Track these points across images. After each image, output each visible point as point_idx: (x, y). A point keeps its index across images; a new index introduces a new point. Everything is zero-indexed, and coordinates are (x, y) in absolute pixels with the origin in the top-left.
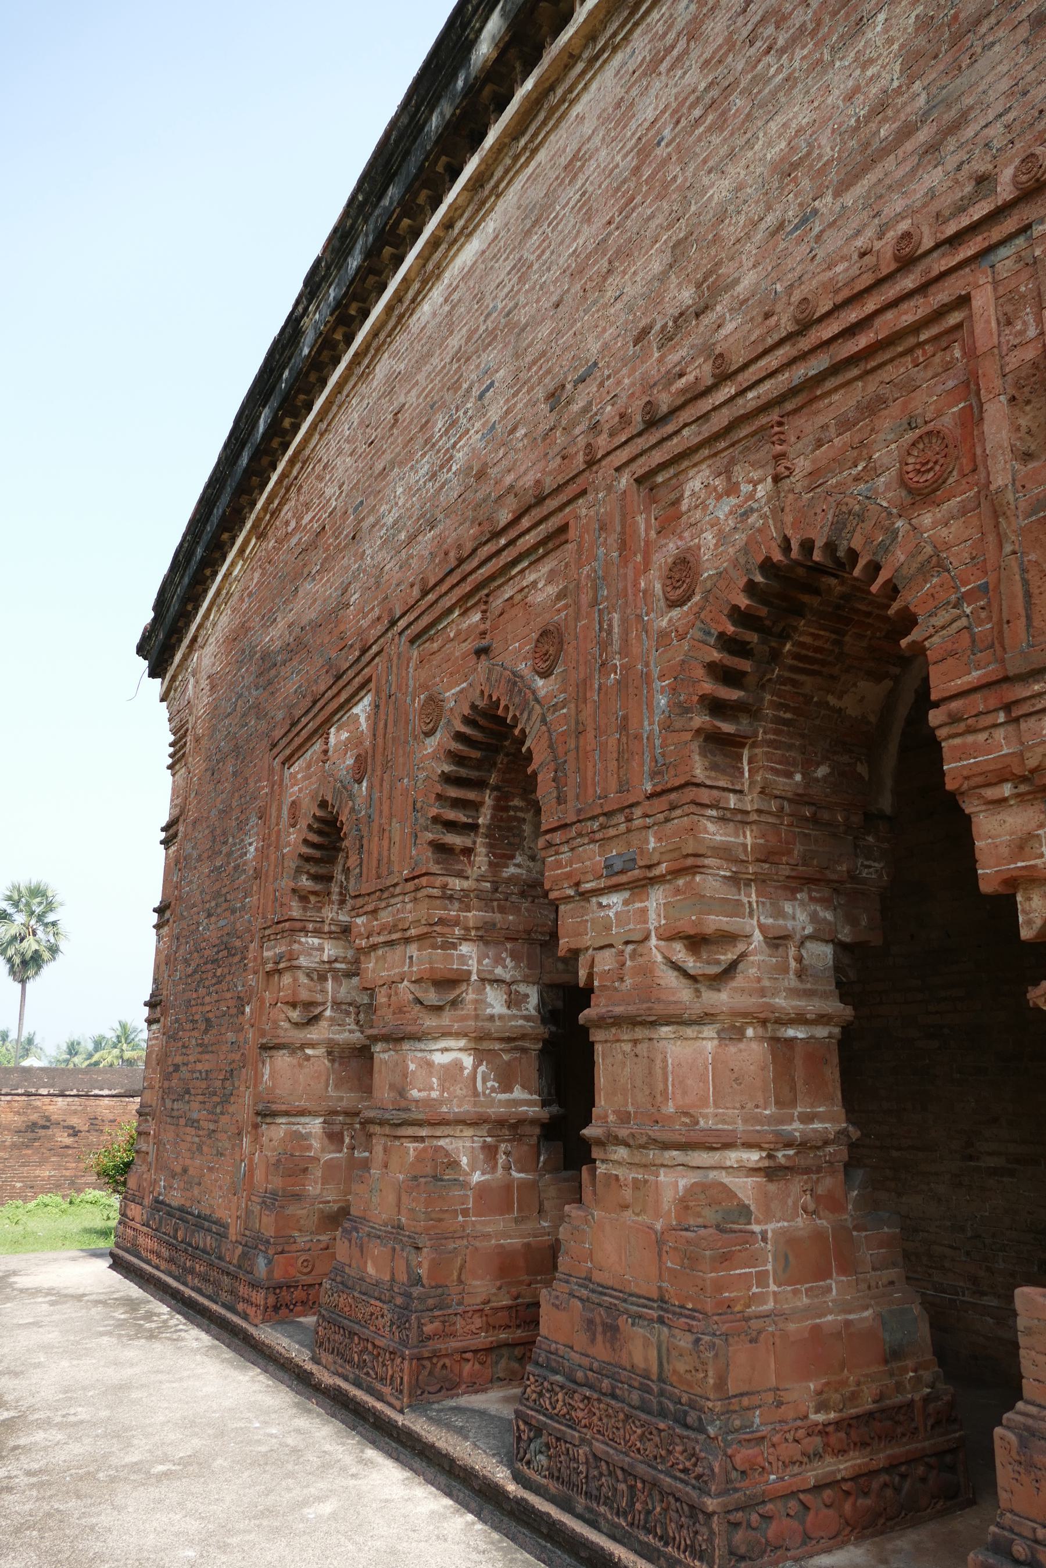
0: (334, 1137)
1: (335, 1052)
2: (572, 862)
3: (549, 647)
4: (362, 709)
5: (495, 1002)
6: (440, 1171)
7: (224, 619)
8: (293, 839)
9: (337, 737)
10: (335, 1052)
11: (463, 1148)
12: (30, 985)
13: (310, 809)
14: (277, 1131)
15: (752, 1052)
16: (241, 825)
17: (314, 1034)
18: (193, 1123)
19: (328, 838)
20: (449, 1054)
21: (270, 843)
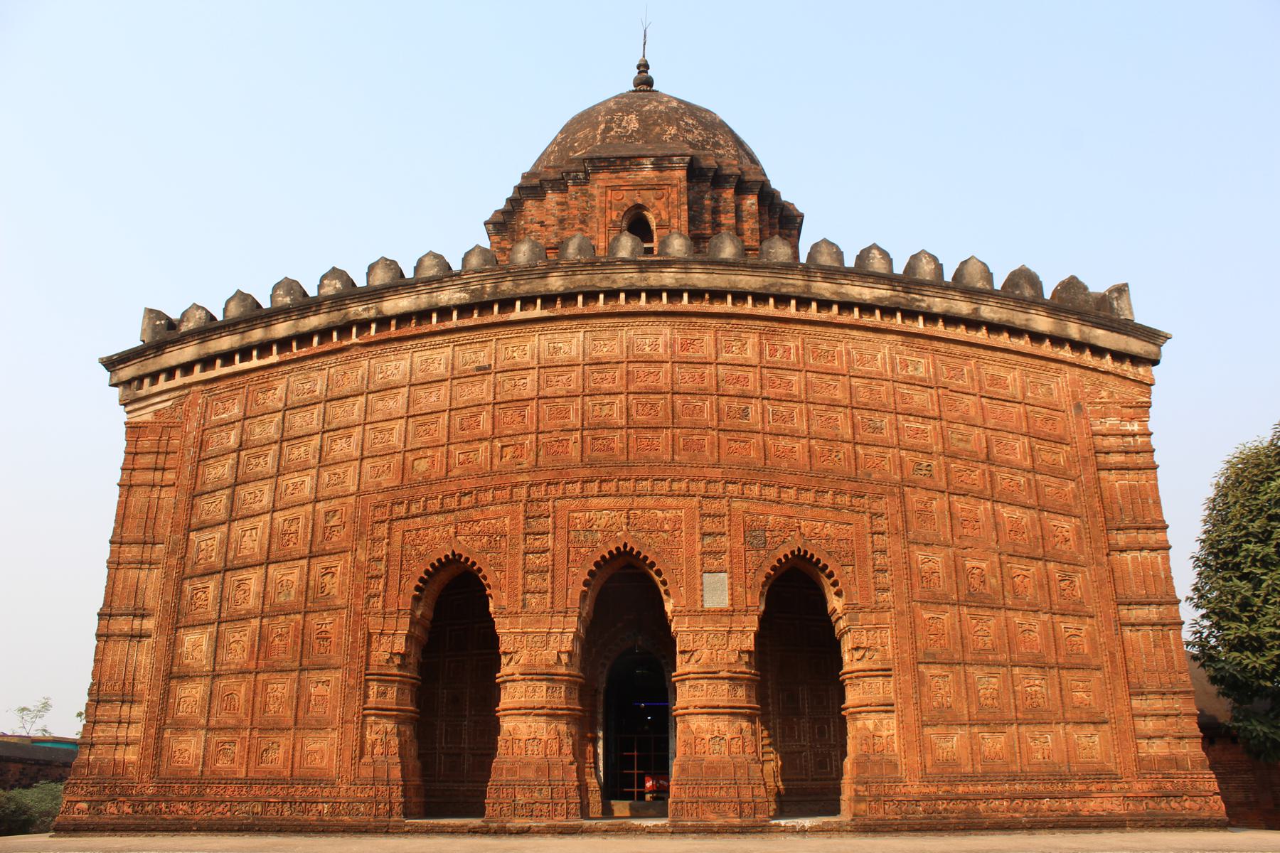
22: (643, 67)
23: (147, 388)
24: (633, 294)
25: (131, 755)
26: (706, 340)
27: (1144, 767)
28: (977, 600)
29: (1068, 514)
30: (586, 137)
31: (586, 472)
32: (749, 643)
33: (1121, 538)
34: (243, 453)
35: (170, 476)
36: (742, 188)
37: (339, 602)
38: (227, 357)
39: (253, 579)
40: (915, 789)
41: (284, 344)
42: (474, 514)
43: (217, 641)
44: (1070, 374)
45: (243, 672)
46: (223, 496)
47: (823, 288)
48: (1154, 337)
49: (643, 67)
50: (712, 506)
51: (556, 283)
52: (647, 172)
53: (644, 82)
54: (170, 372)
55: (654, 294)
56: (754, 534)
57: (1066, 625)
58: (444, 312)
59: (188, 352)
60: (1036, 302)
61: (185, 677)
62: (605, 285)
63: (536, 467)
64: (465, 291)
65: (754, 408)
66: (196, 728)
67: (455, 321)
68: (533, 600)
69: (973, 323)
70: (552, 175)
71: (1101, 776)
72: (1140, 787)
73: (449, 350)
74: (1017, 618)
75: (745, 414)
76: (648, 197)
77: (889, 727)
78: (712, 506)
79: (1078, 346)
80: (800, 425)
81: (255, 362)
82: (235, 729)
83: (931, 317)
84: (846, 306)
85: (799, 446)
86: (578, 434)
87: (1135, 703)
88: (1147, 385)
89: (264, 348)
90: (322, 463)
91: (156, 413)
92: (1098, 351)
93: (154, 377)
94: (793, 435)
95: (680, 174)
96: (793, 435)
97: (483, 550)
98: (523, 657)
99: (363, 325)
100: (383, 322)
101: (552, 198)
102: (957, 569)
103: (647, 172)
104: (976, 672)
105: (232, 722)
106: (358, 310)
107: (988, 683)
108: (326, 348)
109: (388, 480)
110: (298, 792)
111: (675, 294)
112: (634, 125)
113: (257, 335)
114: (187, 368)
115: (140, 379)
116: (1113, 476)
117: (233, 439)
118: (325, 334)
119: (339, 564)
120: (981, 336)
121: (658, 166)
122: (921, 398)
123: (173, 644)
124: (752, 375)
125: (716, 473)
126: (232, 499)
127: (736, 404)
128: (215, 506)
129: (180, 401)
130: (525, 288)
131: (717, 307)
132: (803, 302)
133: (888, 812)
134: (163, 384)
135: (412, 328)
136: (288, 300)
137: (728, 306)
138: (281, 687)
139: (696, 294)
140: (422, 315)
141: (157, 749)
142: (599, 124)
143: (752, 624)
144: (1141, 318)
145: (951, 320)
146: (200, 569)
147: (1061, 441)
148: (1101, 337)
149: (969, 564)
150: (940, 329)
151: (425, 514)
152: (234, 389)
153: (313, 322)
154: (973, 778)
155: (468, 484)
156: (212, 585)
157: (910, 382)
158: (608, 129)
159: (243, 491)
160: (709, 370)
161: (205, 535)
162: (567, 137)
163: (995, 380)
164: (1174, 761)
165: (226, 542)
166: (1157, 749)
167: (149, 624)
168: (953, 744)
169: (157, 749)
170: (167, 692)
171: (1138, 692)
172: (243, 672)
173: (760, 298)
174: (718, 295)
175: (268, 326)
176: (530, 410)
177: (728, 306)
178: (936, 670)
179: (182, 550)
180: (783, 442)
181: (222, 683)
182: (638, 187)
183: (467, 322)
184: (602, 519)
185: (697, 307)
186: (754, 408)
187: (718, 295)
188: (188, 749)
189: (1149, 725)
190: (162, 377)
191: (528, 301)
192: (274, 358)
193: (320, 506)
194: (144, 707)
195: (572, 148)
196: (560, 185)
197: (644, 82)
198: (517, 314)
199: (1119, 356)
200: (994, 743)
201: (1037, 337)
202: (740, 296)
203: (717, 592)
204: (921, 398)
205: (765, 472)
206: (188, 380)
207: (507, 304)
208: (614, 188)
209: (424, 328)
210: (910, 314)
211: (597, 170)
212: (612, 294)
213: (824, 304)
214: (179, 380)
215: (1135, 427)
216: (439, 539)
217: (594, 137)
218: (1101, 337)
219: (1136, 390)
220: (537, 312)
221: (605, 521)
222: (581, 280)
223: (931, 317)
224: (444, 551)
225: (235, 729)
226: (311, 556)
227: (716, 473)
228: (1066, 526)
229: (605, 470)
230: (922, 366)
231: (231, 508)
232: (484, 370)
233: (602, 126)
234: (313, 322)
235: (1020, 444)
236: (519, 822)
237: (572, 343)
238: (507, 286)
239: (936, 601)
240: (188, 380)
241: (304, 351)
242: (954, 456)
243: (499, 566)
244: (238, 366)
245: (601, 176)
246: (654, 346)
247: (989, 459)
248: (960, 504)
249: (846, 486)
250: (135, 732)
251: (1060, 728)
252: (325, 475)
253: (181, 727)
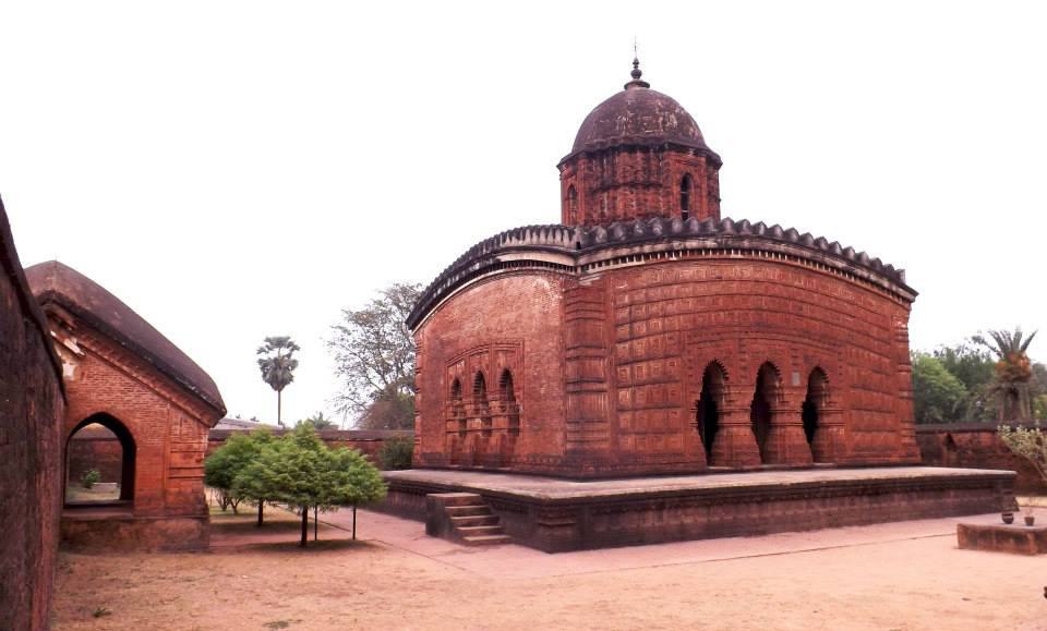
0: (461, 436)
1: (460, 421)
2: (489, 397)
3: (487, 367)
4: (463, 363)
5: (485, 412)
6: (477, 438)
7: (430, 324)
8: (451, 383)
9: (458, 366)
10: (460, 421)
11: (480, 434)
12: (282, 392)
13: (454, 378)
14: (450, 436)
15: (507, 419)
16: (439, 376)
17: (458, 417)
18: (431, 436)
19: (457, 383)
20: (478, 421)
21: (446, 382)
22: (636, 63)
23: (591, 271)
24: (770, 252)
25: (605, 446)
26: (790, 277)
27: (905, 444)
28: (864, 387)
29: (887, 357)
30: (651, 121)
31: (754, 329)
32: (804, 399)
33: (900, 367)
34: (633, 308)
35: (602, 316)
36: (682, 149)
37: (677, 378)
38: (623, 259)
39: (644, 365)
40: (849, 453)
41: (647, 256)
42: (721, 343)
43: (633, 394)
44: (891, 304)
45: (645, 408)
46: (627, 327)
47: (828, 260)
48: (915, 293)
49: (636, 63)
50: (794, 346)
51: (746, 244)
52: (691, 155)
53: (636, 74)
54: (600, 263)
55: (777, 254)
56: (806, 359)
57: (886, 397)
58: (707, 250)
59: (609, 254)
60: (862, 266)
61: (622, 410)
62: (763, 248)
63: (739, 325)
64: (715, 241)
65: (804, 306)
66: (630, 433)
67: (711, 255)
68: (743, 380)
69: (867, 280)
70: (642, 143)
71: (893, 449)
72: (903, 453)
73: (706, 268)
74: (875, 394)
75: (801, 309)
76: (690, 169)
77: (842, 431)
78: (794, 346)
79: (894, 293)
80: (817, 315)
81: (635, 263)
82: (646, 433)
83: (856, 276)
84: (834, 268)
85: (817, 323)
86: (752, 312)
87: (902, 425)
88: (909, 310)
89: (639, 257)
90: (665, 316)
91: (593, 282)
92: (899, 296)
93: (593, 265)
94: (815, 319)
95: (703, 159)
96: (815, 319)
97: (725, 358)
98: (738, 403)
99: (677, 253)
100: (685, 251)
101: (639, 155)
102: (859, 375)
103: (691, 155)
104: (864, 413)
105: (643, 430)
106: (676, 244)
107: (867, 416)
108: (663, 260)
109: (690, 326)
110: (672, 460)
111: (783, 255)
112: (675, 122)
113: (637, 250)
114: (607, 262)
115: (587, 265)
116: (897, 344)
117: (627, 300)
118: (662, 253)
119: (676, 362)
120: (869, 287)
121: (696, 154)
122: (849, 308)
123: (617, 396)
124: (803, 293)
125: (795, 332)
126: (631, 328)
127: (799, 304)
128: (624, 331)
129: (603, 277)
130: (736, 244)
131: (795, 263)
132: (827, 267)
133: (844, 462)
134: (597, 269)
135: (696, 256)
136: (641, 231)
137: (799, 263)
138: (659, 416)
139: (790, 256)
140: (699, 251)
141: (616, 442)
142: (657, 117)
143: (805, 392)
144: (909, 282)
145: (861, 278)
146: (622, 361)
147: (887, 330)
148: (901, 292)
149: (863, 373)
150: (858, 283)
151: (705, 341)
152: (626, 274)
153: (660, 247)
154: (863, 450)
155: (719, 330)
156: (628, 369)
157: (848, 302)
158: (664, 122)
159: (636, 325)
160: (791, 289)
161: (622, 345)
162: (636, 116)
163: (871, 304)
164: (910, 445)
165: (631, 348)
166: (907, 440)
167: (605, 386)
168: (858, 437)
169: (616, 442)
170: (618, 418)
171: (902, 422)
172: (645, 408)
173: (808, 261)
174: (795, 257)
175: (642, 246)
176: (735, 299)
177: (799, 263)
178: (854, 412)
179: (613, 349)
180: (813, 322)
181: (637, 413)
182: (688, 163)
183: (715, 257)
184: (762, 348)
185: (789, 262)
186: (804, 306)
187: (795, 257)
188: (629, 442)
189: (904, 432)
190: (597, 265)
191: (736, 250)
192: (643, 262)
193: (667, 335)
194: (608, 424)
195: (642, 124)
196: (645, 150)
197: (636, 74)
198: (733, 255)
199: (904, 299)
200: (868, 437)
201: (883, 288)
202: (802, 259)
203: (797, 380)
204: (849, 308)
205: (806, 333)
206: (608, 268)
207: (729, 252)
208: (679, 162)
209: (700, 257)
210: (850, 274)
211: (670, 150)
212: (763, 252)
213: (827, 267)
214: (604, 268)
215: (904, 326)
216: (710, 353)
217: (657, 124)
218: (901, 292)
219: (905, 312)
220: (740, 256)
221: (762, 349)
222: (755, 244)
223: (856, 276)
224: (711, 359)
225: (646, 433)
226: (666, 357)
227: (795, 332)
228: (887, 361)
229: (763, 328)
230: (850, 296)
231: (631, 332)
232: (720, 279)
233: (661, 119)
234: (660, 247)
235: (876, 329)
236: (746, 467)
237: (748, 271)
238: (730, 242)
239: (854, 387)
240: (608, 268)
241: (655, 261)
242: (859, 332)
243: (731, 366)
244: (630, 264)
245: (673, 153)
246: (774, 276)
247: (868, 335)
248: (861, 351)
249: (832, 341)
250: (608, 435)
251: (885, 433)
252: (666, 321)
253: (624, 432)
